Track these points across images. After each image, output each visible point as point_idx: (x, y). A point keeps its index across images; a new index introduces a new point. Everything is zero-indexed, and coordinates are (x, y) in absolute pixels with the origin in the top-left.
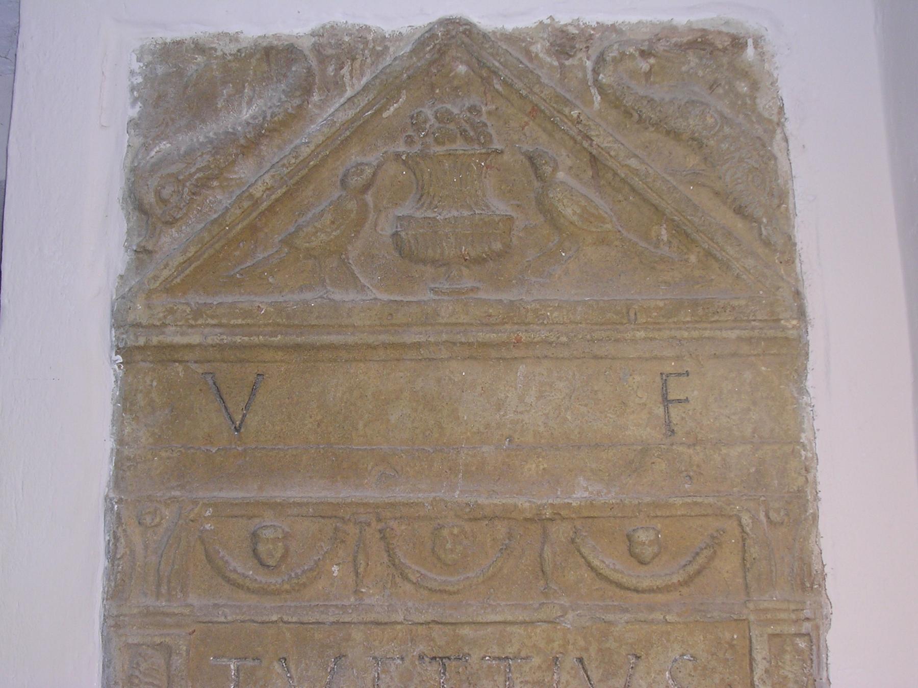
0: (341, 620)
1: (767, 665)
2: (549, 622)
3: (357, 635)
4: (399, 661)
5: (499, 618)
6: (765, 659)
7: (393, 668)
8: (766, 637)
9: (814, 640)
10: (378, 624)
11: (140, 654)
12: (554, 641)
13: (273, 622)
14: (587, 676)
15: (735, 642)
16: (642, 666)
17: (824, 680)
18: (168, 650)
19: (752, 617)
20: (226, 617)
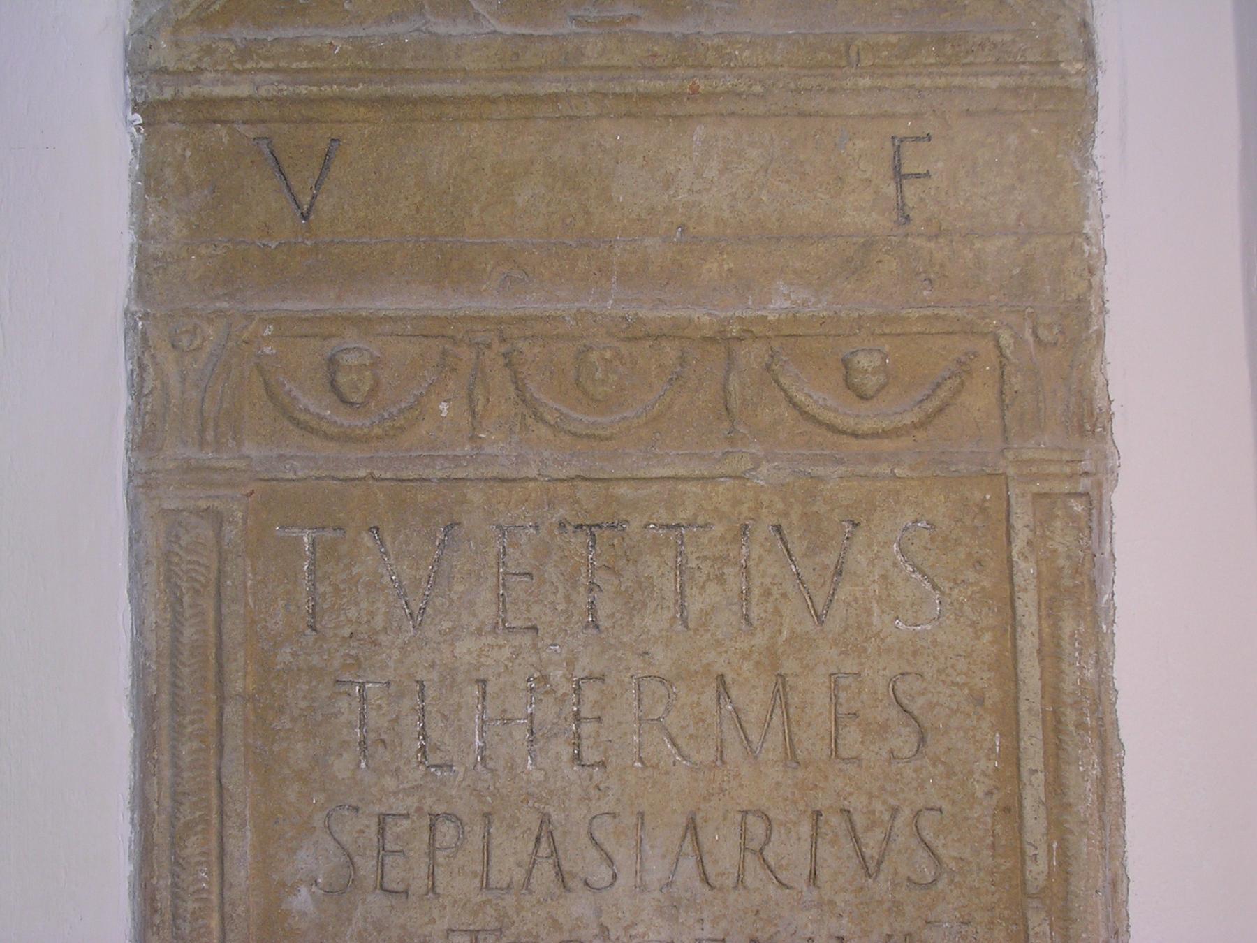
1: (1030, 535)
2: (735, 477)
3: (476, 496)
4: (532, 531)
6: (1027, 526)
7: (524, 540)
8: (1029, 497)
9: (1095, 502)
10: (503, 480)
11: (180, 524)
15: (987, 504)
16: (861, 536)
17: (1107, 555)
18: (218, 519)
19: (1011, 471)
20: (295, 473)
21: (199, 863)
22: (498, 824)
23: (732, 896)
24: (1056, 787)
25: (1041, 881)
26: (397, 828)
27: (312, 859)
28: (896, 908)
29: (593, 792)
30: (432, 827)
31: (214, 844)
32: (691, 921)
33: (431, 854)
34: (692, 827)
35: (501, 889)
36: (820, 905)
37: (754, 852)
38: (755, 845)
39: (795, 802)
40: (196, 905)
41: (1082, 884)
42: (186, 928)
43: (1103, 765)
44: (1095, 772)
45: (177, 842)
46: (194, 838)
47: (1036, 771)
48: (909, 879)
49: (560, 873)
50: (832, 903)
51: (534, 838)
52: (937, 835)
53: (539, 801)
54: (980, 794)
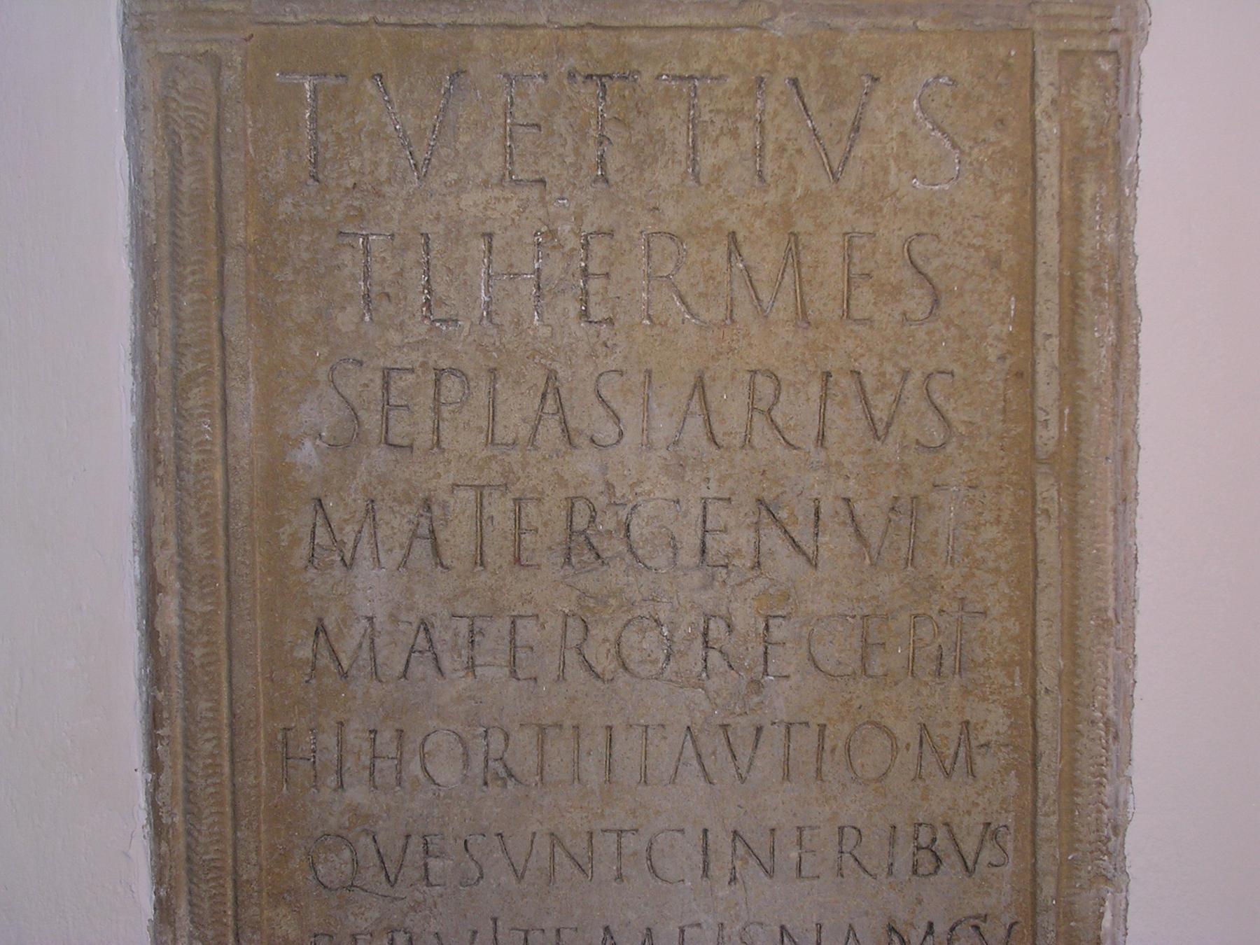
0: (459, 21)
1: (1055, 93)
2: (751, 27)
3: (482, 42)
4: (540, 80)
5: (681, 21)
6: (1052, 84)
7: (532, 89)
8: (1055, 54)
9: (1123, 61)
10: (511, 27)
11: (177, 68)
12: (758, 54)
13: (362, 24)
14: (804, 104)
15: (1011, 61)
16: (880, 93)
17: (1133, 116)
18: (216, 64)
19: (1038, 26)
20: (296, 16)
21: (201, 415)
22: (503, 380)
23: (739, 456)
24: (1071, 351)
25: (1051, 447)
26: (401, 382)
27: (316, 413)
28: (904, 471)
29: (601, 350)
30: (437, 382)
31: (217, 397)
32: (697, 480)
33: (437, 411)
34: (700, 386)
35: (507, 445)
36: (827, 466)
37: (762, 412)
38: (763, 406)
39: (804, 362)
40: (200, 457)
41: (1092, 450)
42: (190, 479)
43: (1119, 330)
44: (1111, 339)
45: (179, 394)
46: (196, 390)
47: (1050, 336)
48: (918, 442)
49: (566, 430)
50: (839, 464)
51: (540, 394)
52: (947, 398)
53: (545, 357)
54: (992, 358)
